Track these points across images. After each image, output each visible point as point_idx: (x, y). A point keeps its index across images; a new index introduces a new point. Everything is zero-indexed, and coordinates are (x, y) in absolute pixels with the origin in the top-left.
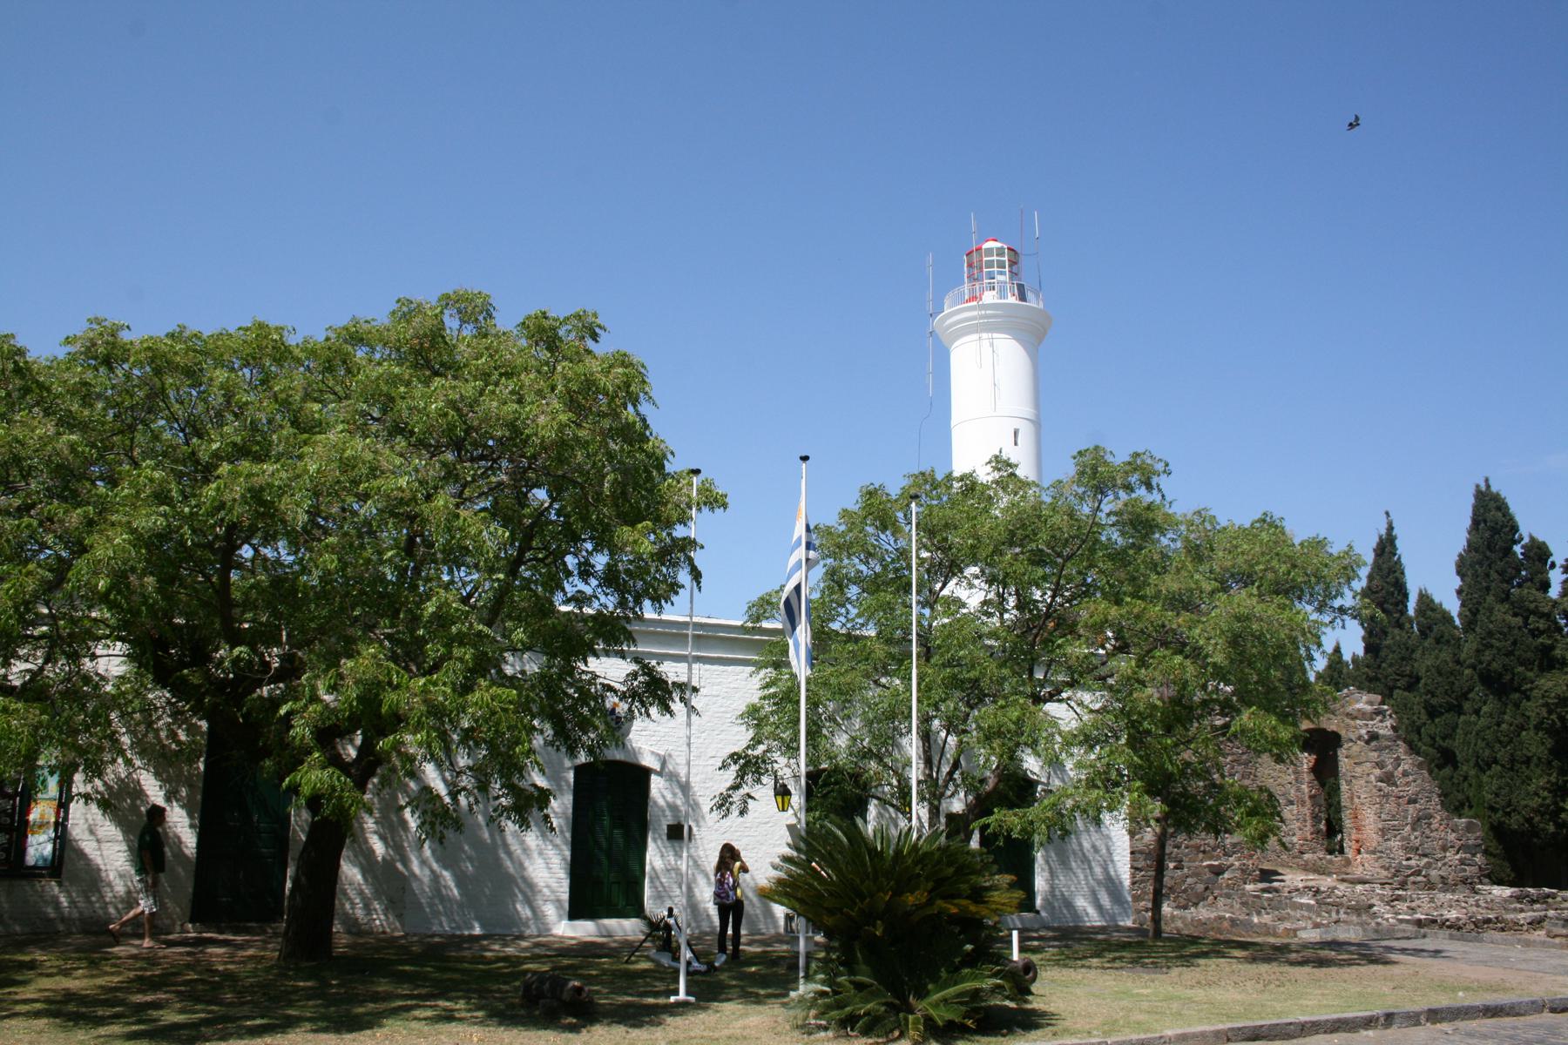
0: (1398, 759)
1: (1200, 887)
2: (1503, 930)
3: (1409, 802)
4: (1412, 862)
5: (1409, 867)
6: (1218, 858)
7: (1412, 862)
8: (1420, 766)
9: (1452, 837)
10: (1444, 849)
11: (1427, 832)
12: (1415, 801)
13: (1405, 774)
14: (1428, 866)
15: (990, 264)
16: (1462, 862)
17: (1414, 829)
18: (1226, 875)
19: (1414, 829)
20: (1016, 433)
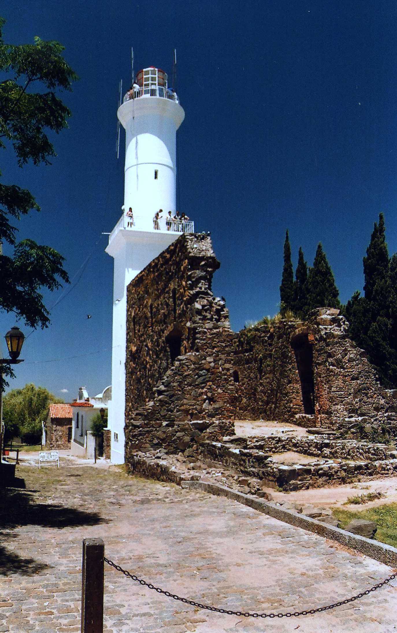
1: (187, 439)
2: (371, 474)
3: (353, 379)
4: (353, 419)
5: (350, 422)
6: (203, 418)
7: (353, 419)
8: (362, 355)
9: (382, 402)
10: (377, 409)
11: (365, 399)
12: (357, 379)
13: (351, 360)
14: (364, 421)
15: (147, 79)
17: (355, 397)
18: (208, 430)
19: (355, 397)
20: (156, 173)
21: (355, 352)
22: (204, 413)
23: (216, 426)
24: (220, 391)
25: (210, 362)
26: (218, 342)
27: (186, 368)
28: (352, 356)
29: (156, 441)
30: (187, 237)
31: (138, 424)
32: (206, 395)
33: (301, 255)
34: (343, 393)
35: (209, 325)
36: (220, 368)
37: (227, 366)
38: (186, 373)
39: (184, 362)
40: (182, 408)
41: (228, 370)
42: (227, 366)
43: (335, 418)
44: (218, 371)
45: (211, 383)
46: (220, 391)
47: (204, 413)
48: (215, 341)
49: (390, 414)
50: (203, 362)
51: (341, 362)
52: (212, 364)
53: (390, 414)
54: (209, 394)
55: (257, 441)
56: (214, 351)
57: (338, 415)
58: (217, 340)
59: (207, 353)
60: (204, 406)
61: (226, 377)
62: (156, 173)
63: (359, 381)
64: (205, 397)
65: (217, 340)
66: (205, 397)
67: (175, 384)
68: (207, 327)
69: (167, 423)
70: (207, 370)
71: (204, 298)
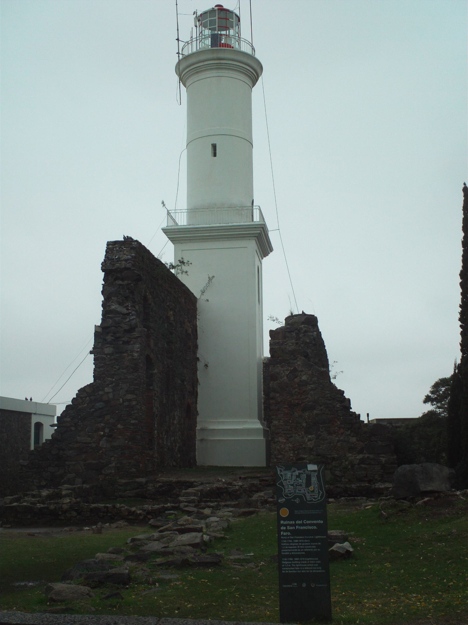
0: (295, 370)
16: (362, 461)
20: (214, 147)
22: (101, 452)
25: (108, 393)
26: (118, 369)
28: (304, 378)
31: (26, 464)
32: (104, 431)
36: (121, 400)
37: (129, 396)
38: (80, 407)
41: (130, 400)
42: (129, 396)
46: (119, 426)
47: (101, 452)
48: (115, 368)
49: (366, 456)
50: (101, 393)
52: (111, 396)
55: (160, 486)
56: (114, 380)
58: (117, 367)
60: (101, 443)
62: (214, 147)
63: (315, 412)
64: (102, 433)
65: (117, 367)
66: (102, 433)
67: (69, 419)
68: (106, 352)
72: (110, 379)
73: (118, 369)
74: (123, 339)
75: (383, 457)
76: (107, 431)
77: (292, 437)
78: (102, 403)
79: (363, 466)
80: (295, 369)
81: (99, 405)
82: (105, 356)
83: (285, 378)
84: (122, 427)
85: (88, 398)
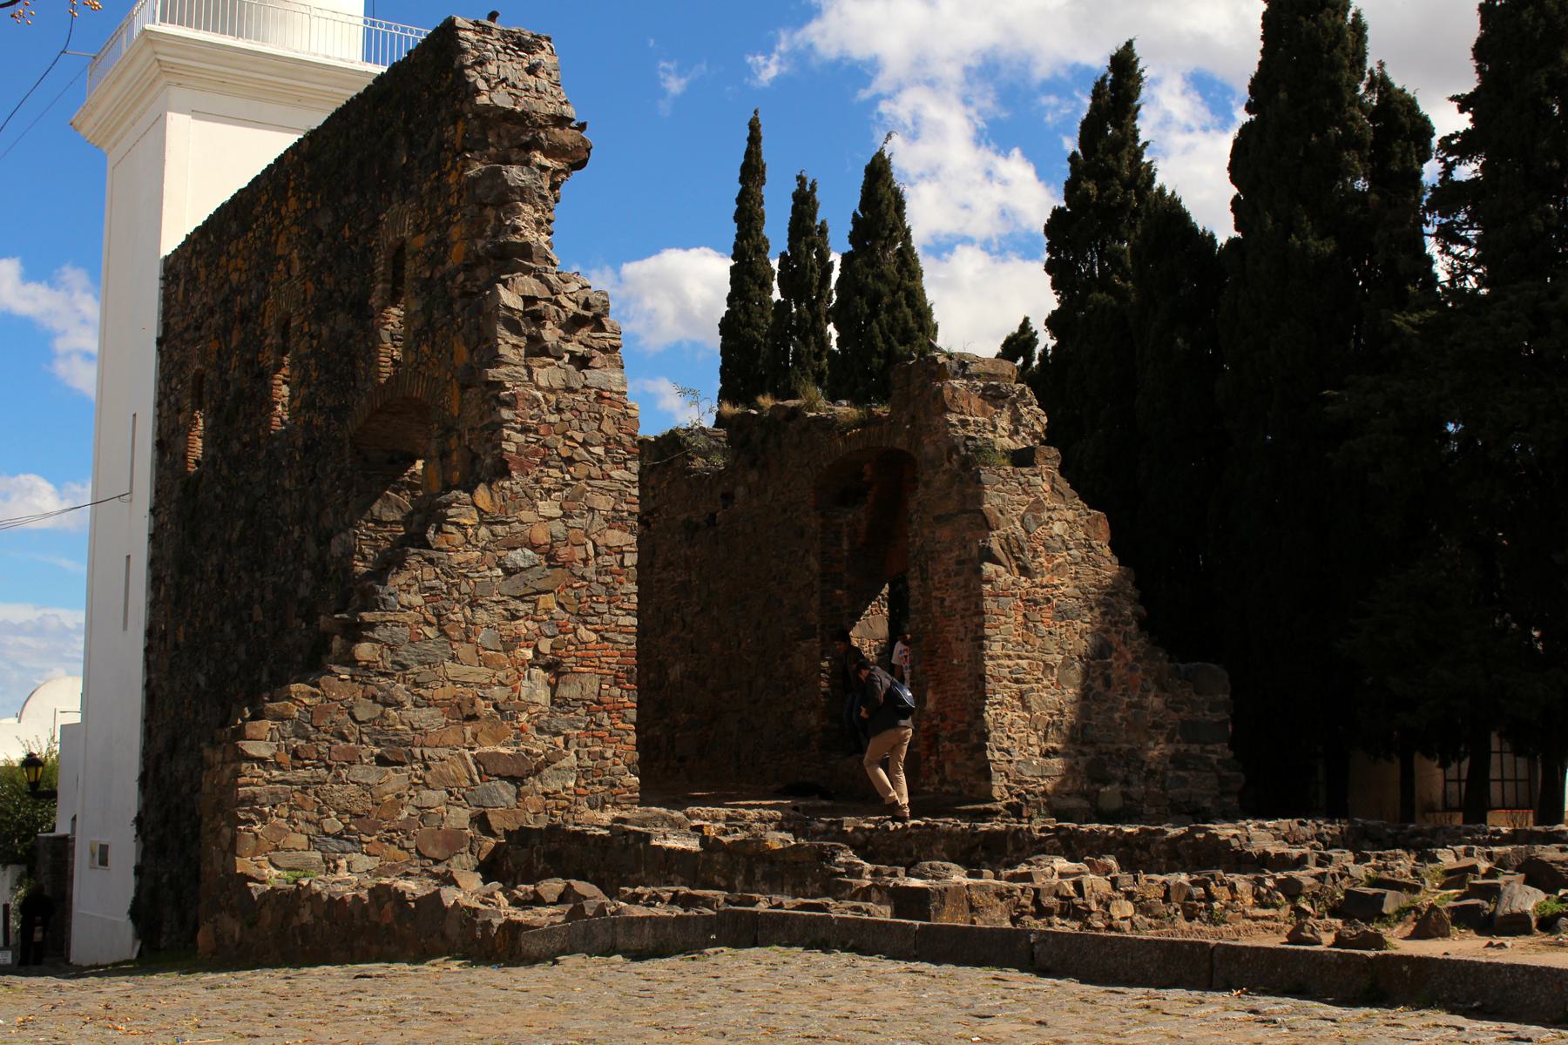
0: (1037, 506)
1: (460, 817)
16: (1178, 761)
21: (1070, 515)
22: (524, 717)
23: (571, 769)
24: (582, 631)
27: (458, 537)
28: (1058, 528)
29: (333, 824)
30: (461, 34)
33: (804, 201)
34: (1024, 663)
35: (548, 374)
36: (590, 546)
39: (450, 512)
40: (440, 693)
42: (616, 537)
43: (997, 755)
44: (579, 553)
45: (547, 601)
48: (571, 439)
49: (1182, 747)
50: (526, 515)
51: (1022, 550)
52: (558, 528)
53: (1182, 747)
54: (545, 646)
57: (1006, 744)
59: (537, 481)
61: (608, 579)
65: (579, 437)
67: (418, 600)
68: (543, 383)
69: (377, 751)
70: (534, 547)
71: (528, 271)
72: (555, 473)
73: (584, 444)
74: (569, 347)
75: (1213, 752)
76: (545, 646)
77: (1032, 690)
78: (528, 552)
79: (1181, 773)
80: (1038, 501)
81: (519, 557)
82: (539, 394)
83: (1018, 524)
84: (594, 636)
85: (483, 531)
